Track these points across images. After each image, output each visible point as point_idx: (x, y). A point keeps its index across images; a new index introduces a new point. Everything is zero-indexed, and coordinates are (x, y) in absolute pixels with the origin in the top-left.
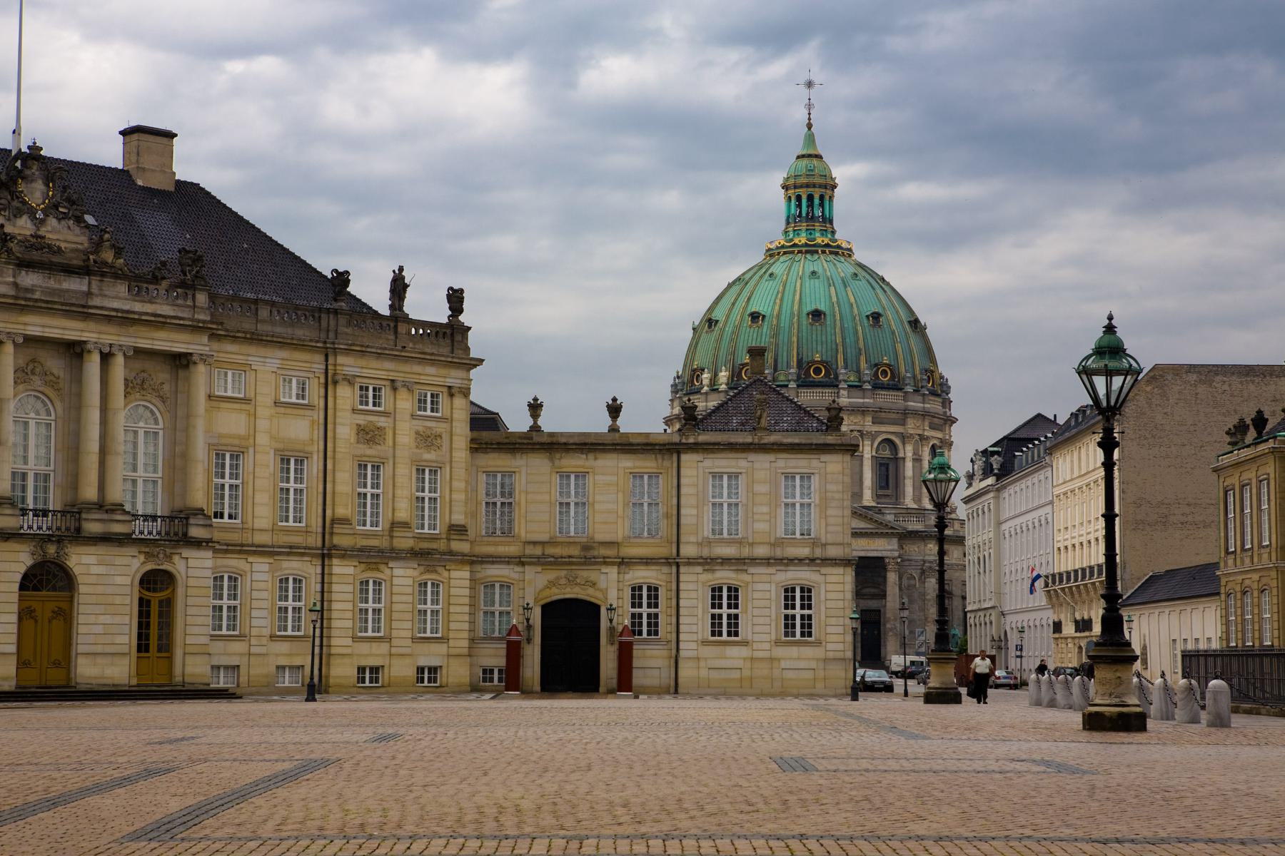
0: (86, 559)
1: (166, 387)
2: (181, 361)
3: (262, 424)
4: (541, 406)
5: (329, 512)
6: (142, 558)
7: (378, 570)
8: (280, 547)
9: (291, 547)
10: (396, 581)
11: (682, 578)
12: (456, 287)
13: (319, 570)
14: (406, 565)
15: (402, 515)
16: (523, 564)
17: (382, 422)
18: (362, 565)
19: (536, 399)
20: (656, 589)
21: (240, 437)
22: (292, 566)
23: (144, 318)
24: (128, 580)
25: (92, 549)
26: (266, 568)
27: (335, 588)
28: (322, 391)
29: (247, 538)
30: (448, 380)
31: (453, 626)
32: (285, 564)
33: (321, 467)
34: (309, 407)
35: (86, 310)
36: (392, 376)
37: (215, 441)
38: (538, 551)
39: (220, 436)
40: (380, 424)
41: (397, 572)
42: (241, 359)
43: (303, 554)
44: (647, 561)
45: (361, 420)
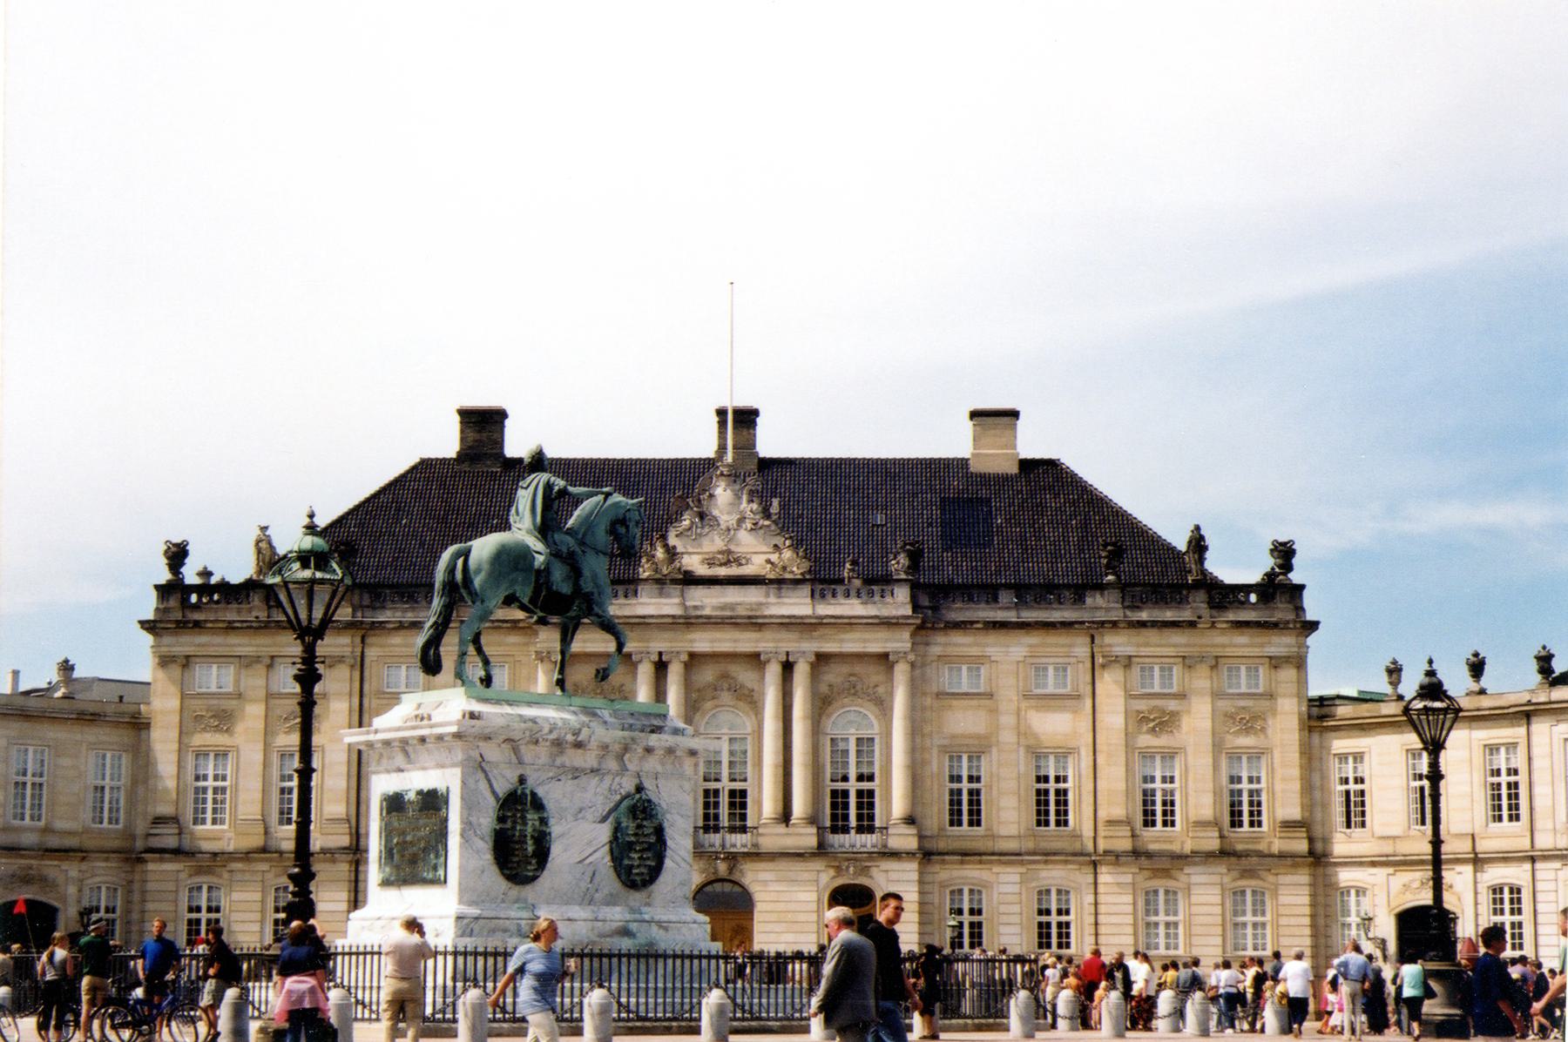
0: (763, 876)
1: (881, 690)
2: (884, 659)
3: (1007, 720)
4: (1400, 670)
5: (1102, 814)
6: (832, 872)
7: (1171, 877)
11: (1539, 875)
12: (1282, 539)
13: (1090, 879)
14: (1210, 870)
16: (1373, 864)
17: (1172, 705)
18: (1146, 872)
19: (1395, 662)
20: (1519, 891)
21: (978, 737)
22: (1054, 875)
23: (825, 621)
24: (814, 896)
25: (770, 865)
26: (1017, 878)
28: (1088, 678)
29: (988, 845)
30: (1267, 649)
32: (1044, 874)
35: (754, 621)
36: (1183, 651)
37: (946, 742)
38: (1387, 848)
39: (953, 737)
40: (1170, 708)
42: (974, 651)
43: (1066, 862)
44: (1506, 858)
45: (1143, 705)
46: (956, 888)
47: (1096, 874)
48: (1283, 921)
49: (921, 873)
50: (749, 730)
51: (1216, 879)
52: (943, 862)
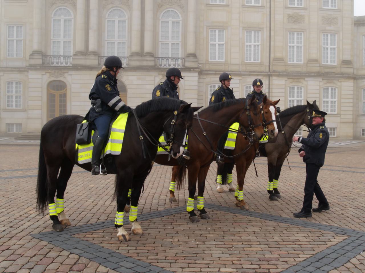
5: (272, 56)
8: (245, 72)
9: (250, 72)
10: (309, 87)
15: (314, 56)
17: (302, 12)
26: (238, 81)
27: (274, 90)
31: (343, 108)
33: (268, 35)
34: (262, 7)
41: (309, 83)
45: (290, 12)
46: (213, 85)
47: (269, 80)
48: (343, 100)
49: (199, 78)
50: (127, 17)
51: (318, 83)
52: (208, 74)
